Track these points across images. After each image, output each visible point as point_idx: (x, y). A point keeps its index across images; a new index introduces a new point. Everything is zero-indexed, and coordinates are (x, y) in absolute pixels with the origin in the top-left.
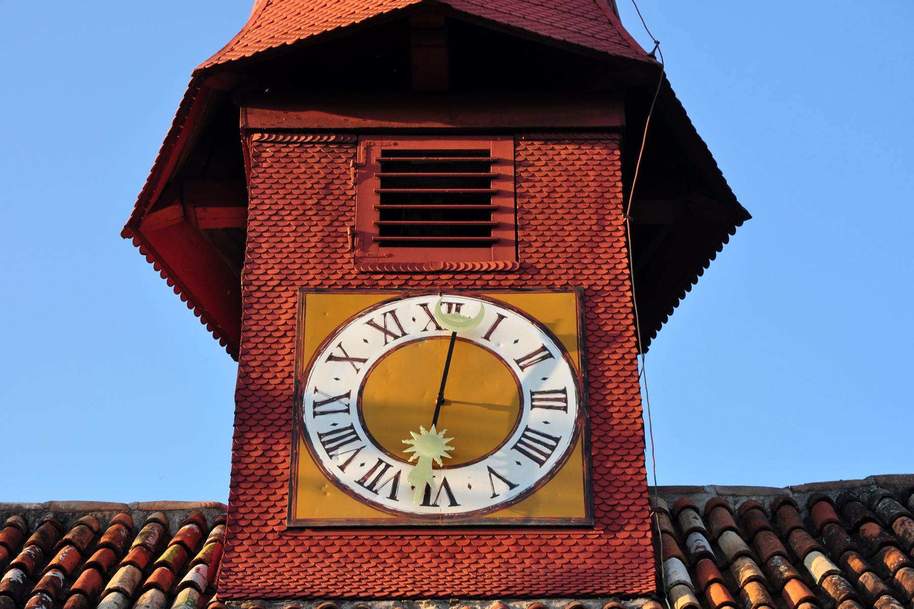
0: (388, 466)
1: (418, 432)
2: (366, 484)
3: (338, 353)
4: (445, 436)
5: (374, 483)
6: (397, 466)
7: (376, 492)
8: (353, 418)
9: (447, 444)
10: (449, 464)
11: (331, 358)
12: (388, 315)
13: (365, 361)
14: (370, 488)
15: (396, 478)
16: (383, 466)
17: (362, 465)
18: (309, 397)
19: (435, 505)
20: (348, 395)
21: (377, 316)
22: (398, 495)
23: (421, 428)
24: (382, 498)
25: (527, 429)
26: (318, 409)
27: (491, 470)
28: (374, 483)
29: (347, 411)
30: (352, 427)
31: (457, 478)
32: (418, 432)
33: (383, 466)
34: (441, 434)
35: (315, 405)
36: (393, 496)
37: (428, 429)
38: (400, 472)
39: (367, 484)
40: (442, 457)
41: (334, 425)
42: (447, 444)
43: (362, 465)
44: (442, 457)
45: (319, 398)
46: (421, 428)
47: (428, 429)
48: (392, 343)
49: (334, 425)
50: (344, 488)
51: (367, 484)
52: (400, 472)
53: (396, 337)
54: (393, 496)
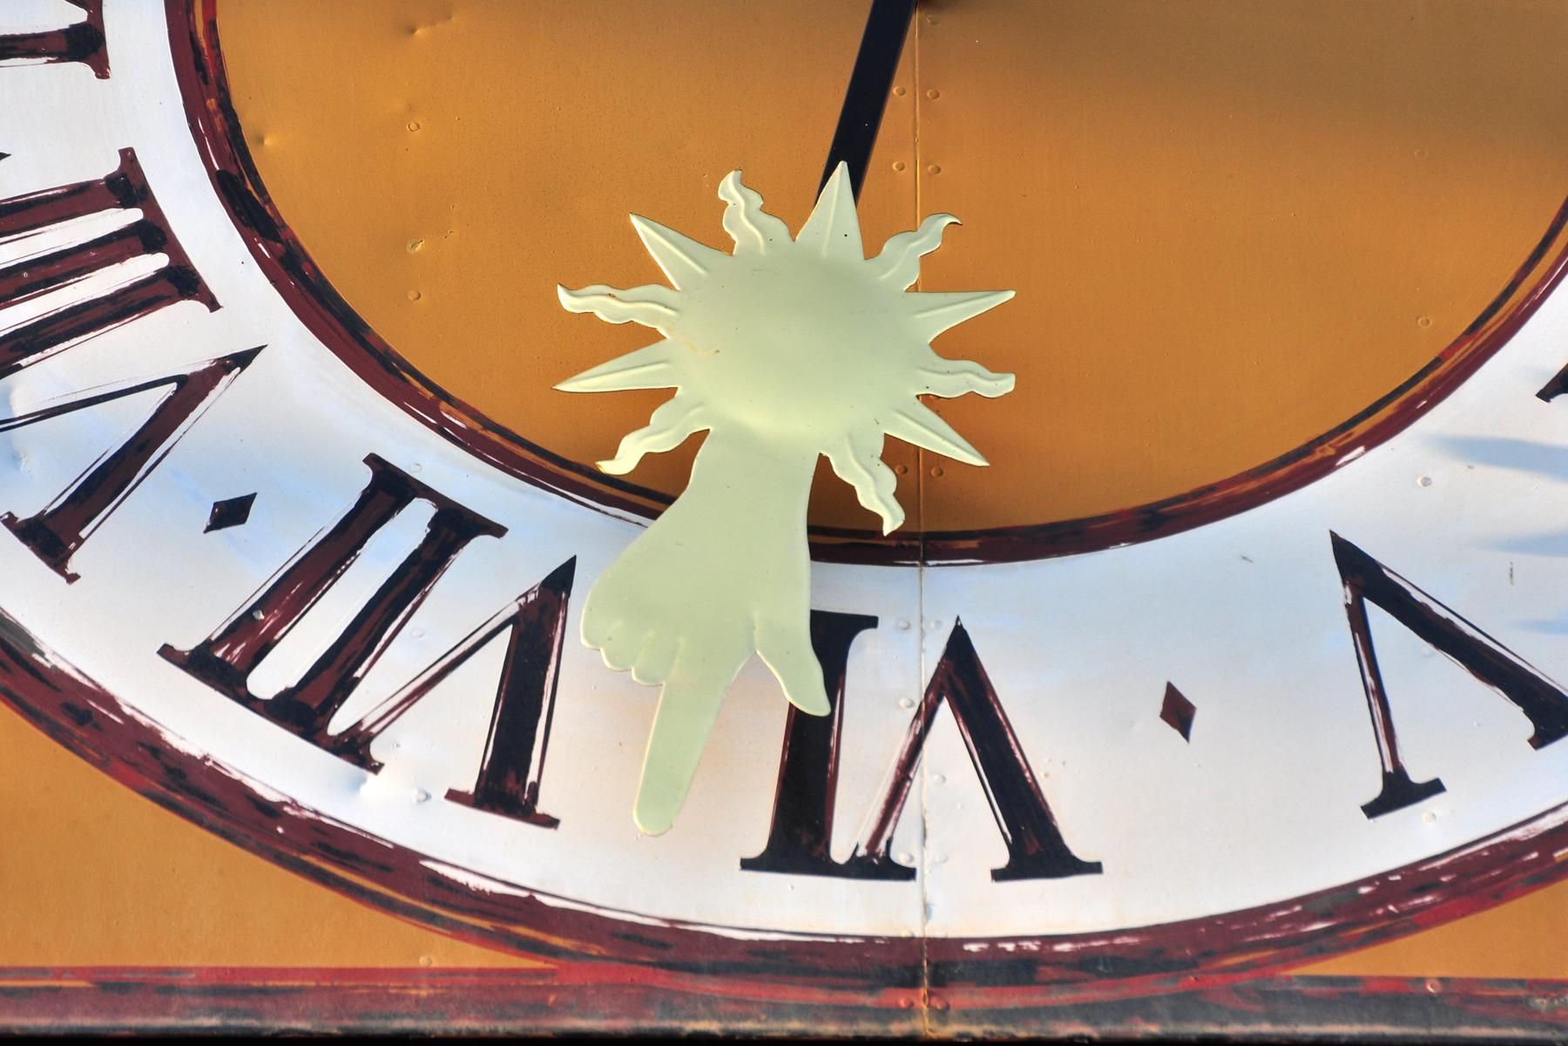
0: (456, 526)
1: (705, 228)
2: (268, 680)
4: (937, 277)
5: (338, 670)
6: (535, 527)
7: (355, 748)
9: (949, 346)
10: (949, 526)
14: (302, 711)
15: (535, 632)
16: (406, 531)
17: (231, 513)
22: (557, 772)
23: (729, 188)
28: (338, 670)
32: (705, 228)
33: (406, 531)
34: (905, 255)
36: (505, 787)
37: (791, 208)
38: (560, 582)
39: (274, 675)
40: (896, 453)
42: (949, 346)
43: (231, 513)
44: (896, 453)
46: (729, 188)
47: (791, 208)
50: (79, 717)
51: (274, 675)
52: (560, 582)
54: (505, 787)
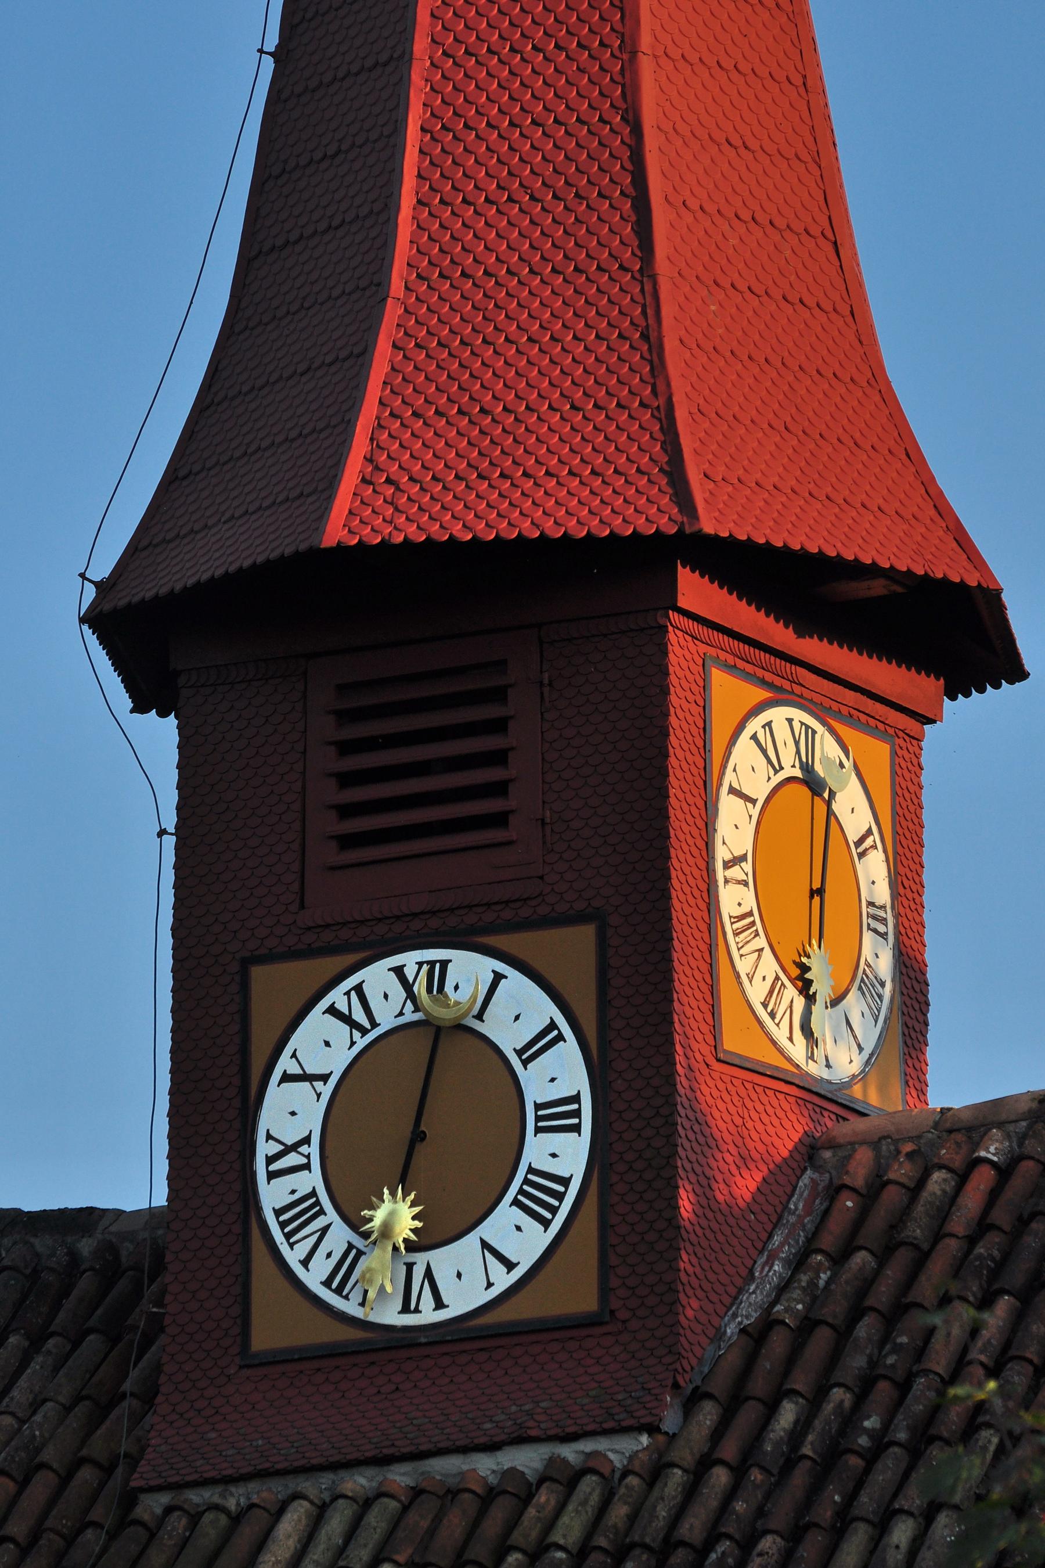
3: (294, 1069)
8: (312, 1180)
11: (286, 1078)
12: (353, 993)
13: (325, 1078)
14: (339, 1291)
18: (264, 1149)
19: (417, 1310)
20: (307, 1140)
21: (337, 997)
24: (350, 1307)
25: (531, 1170)
26: (275, 1167)
27: (485, 1245)
29: (307, 1167)
30: (313, 1193)
31: (442, 1260)
35: (270, 1160)
41: (293, 1192)
45: (274, 1148)
48: (362, 1042)
49: (293, 1192)
53: (364, 1032)
